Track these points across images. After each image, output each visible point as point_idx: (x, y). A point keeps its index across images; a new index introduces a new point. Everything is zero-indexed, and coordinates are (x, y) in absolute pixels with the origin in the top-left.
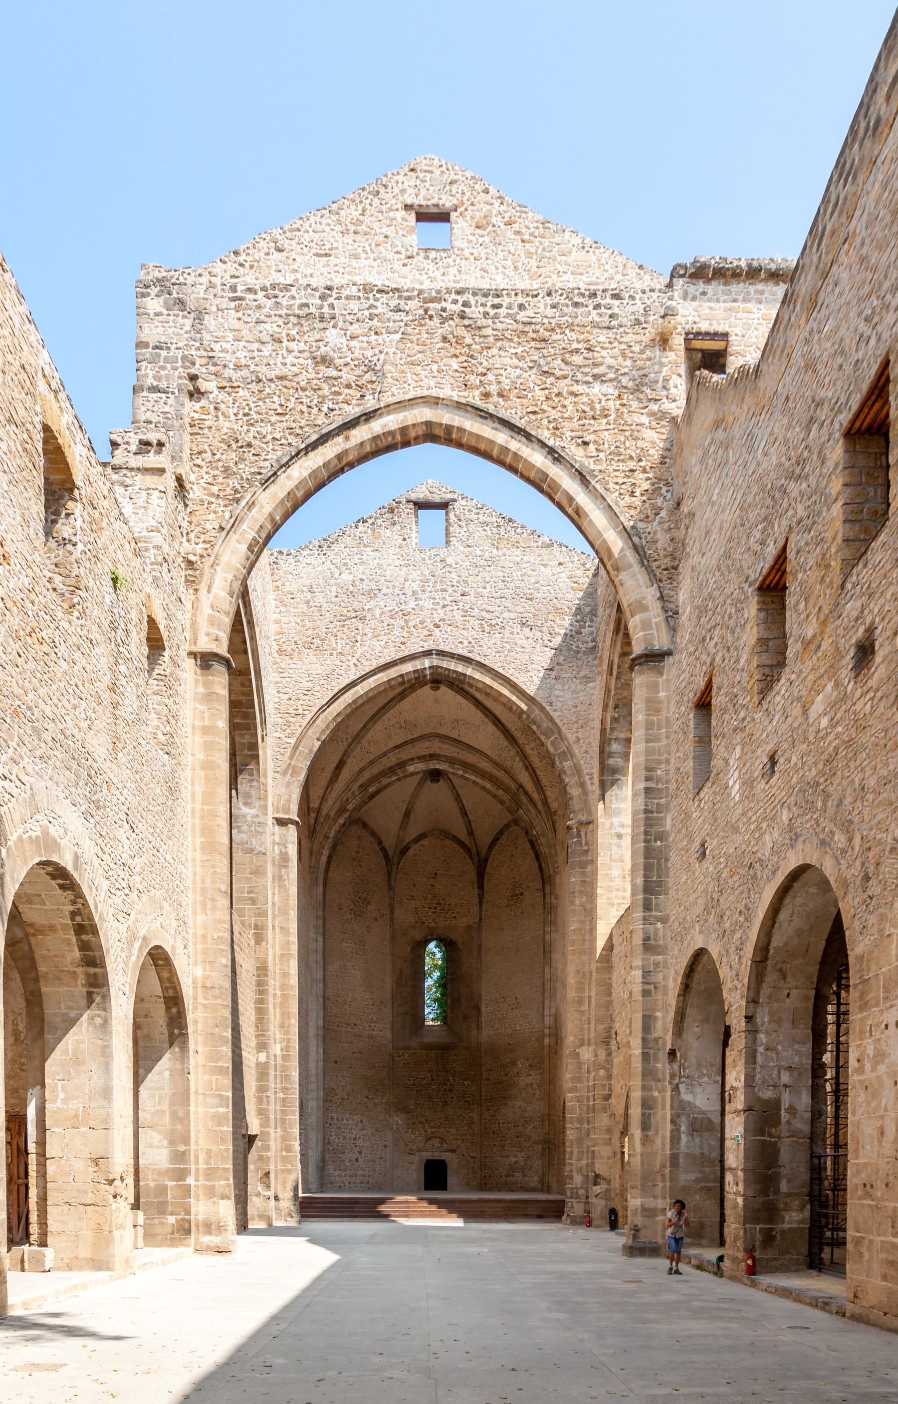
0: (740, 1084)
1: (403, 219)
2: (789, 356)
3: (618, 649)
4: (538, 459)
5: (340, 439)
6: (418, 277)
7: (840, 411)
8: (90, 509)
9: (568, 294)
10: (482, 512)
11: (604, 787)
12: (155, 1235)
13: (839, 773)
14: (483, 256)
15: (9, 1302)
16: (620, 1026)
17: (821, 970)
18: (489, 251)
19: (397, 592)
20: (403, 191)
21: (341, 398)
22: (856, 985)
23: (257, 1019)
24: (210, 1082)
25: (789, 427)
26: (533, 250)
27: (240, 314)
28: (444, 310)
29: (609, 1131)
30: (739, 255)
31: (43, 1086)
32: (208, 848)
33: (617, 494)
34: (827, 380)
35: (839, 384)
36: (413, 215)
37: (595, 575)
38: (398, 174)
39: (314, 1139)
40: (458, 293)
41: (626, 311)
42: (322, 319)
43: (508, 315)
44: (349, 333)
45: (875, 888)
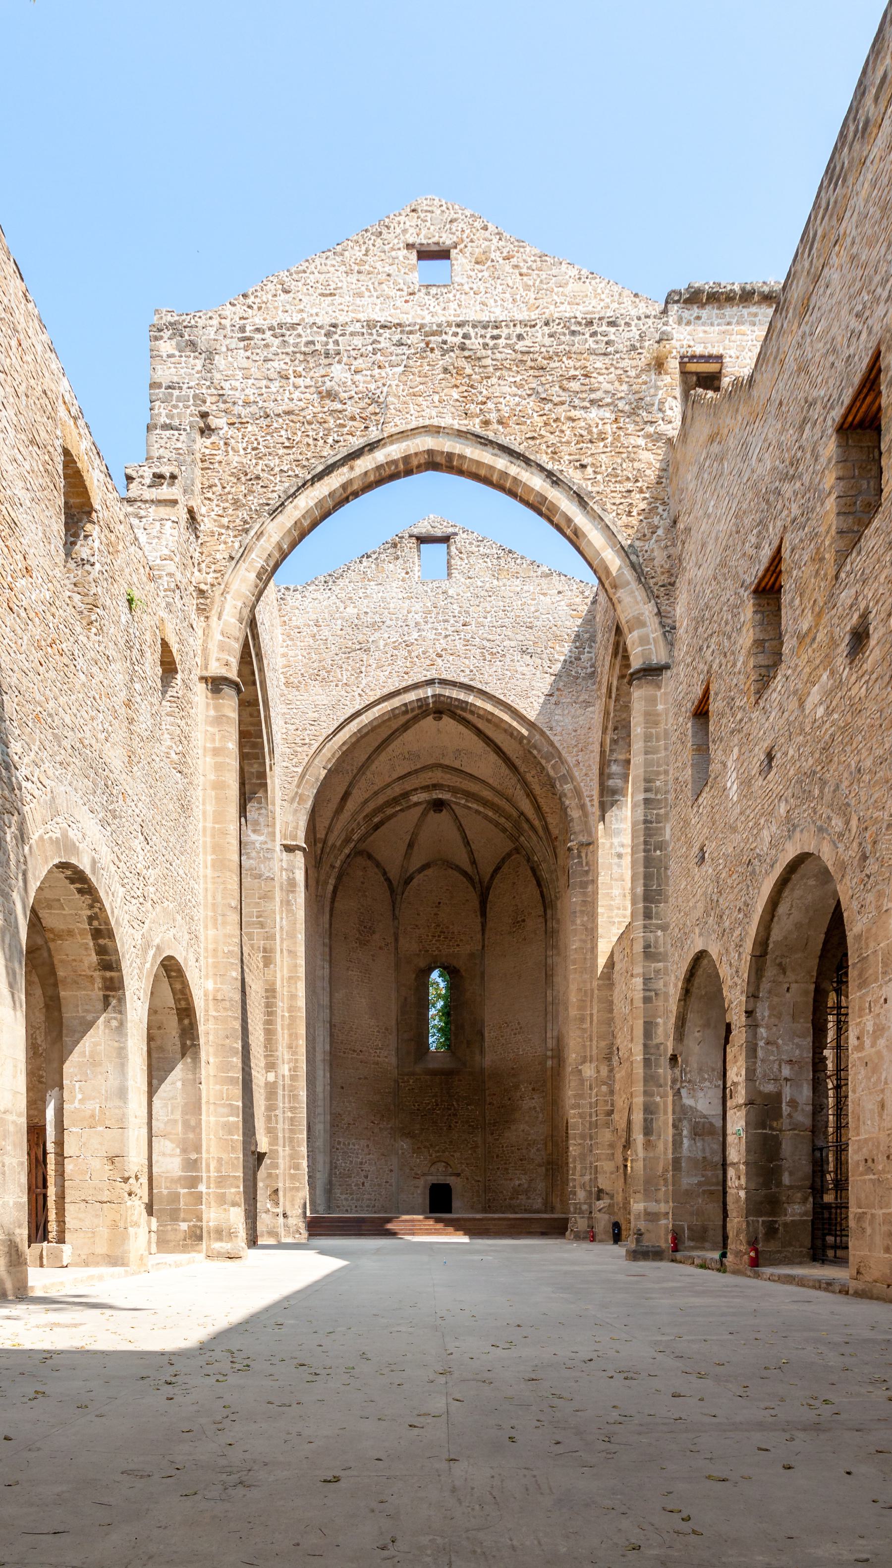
0: (741, 1079)
1: (405, 258)
2: (782, 362)
3: (617, 672)
4: (537, 482)
5: (345, 469)
6: (419, 312)
7: (832, 407)
8: (107, 532)
9: (565, 322)
10: (482, 544)
11: (604, 808)
12: (168, 1242)
13: (836, 759)
14: (483, 290)
15: (30, 1284)
16: (621, 1041)
17: (820, 965)
18: (488, 285)
19: (400, 623)
21: (345, 430)
22: (854, 964)
23: (266, 1039)
24: (221, 1091)
25: (783, 430)
26: (531, 283)
27: (249, 354)
28: (445, 342)
29: (612, 1146)
30: (733, 279)
31: (61, 1088)
32: (219, 865)
33: (614, 514)
34: (819, 380)
35: (831, 382)
36: (415, 253)
37: (594, 602)
38: (400, 215)
39: (321, 1162)
40: (458, 325)
41: (621, 337)
42: (327, 355)
43: (507, 346)
44: (353, 368)
45: (872, 866)
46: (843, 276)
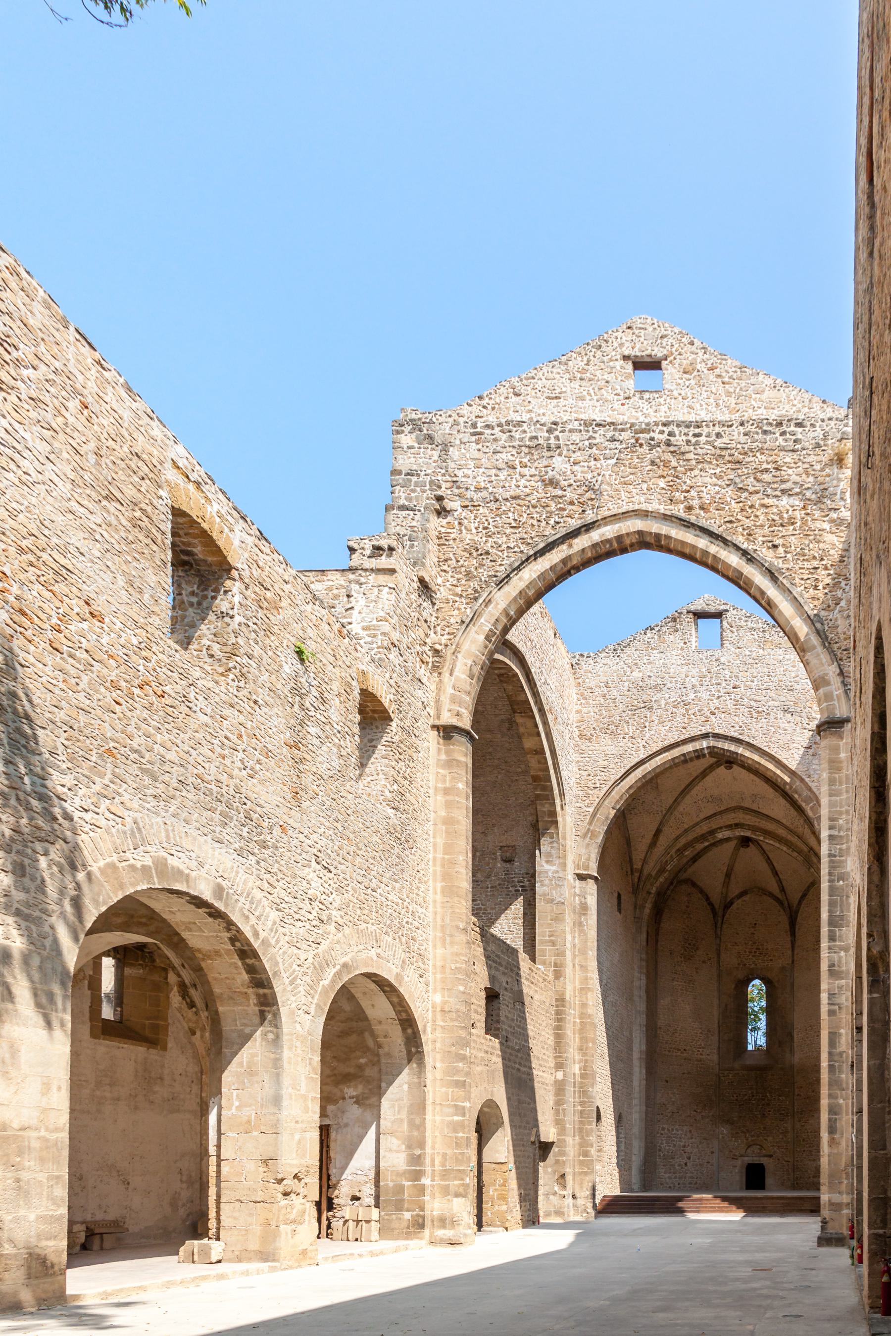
14: (690, 395)
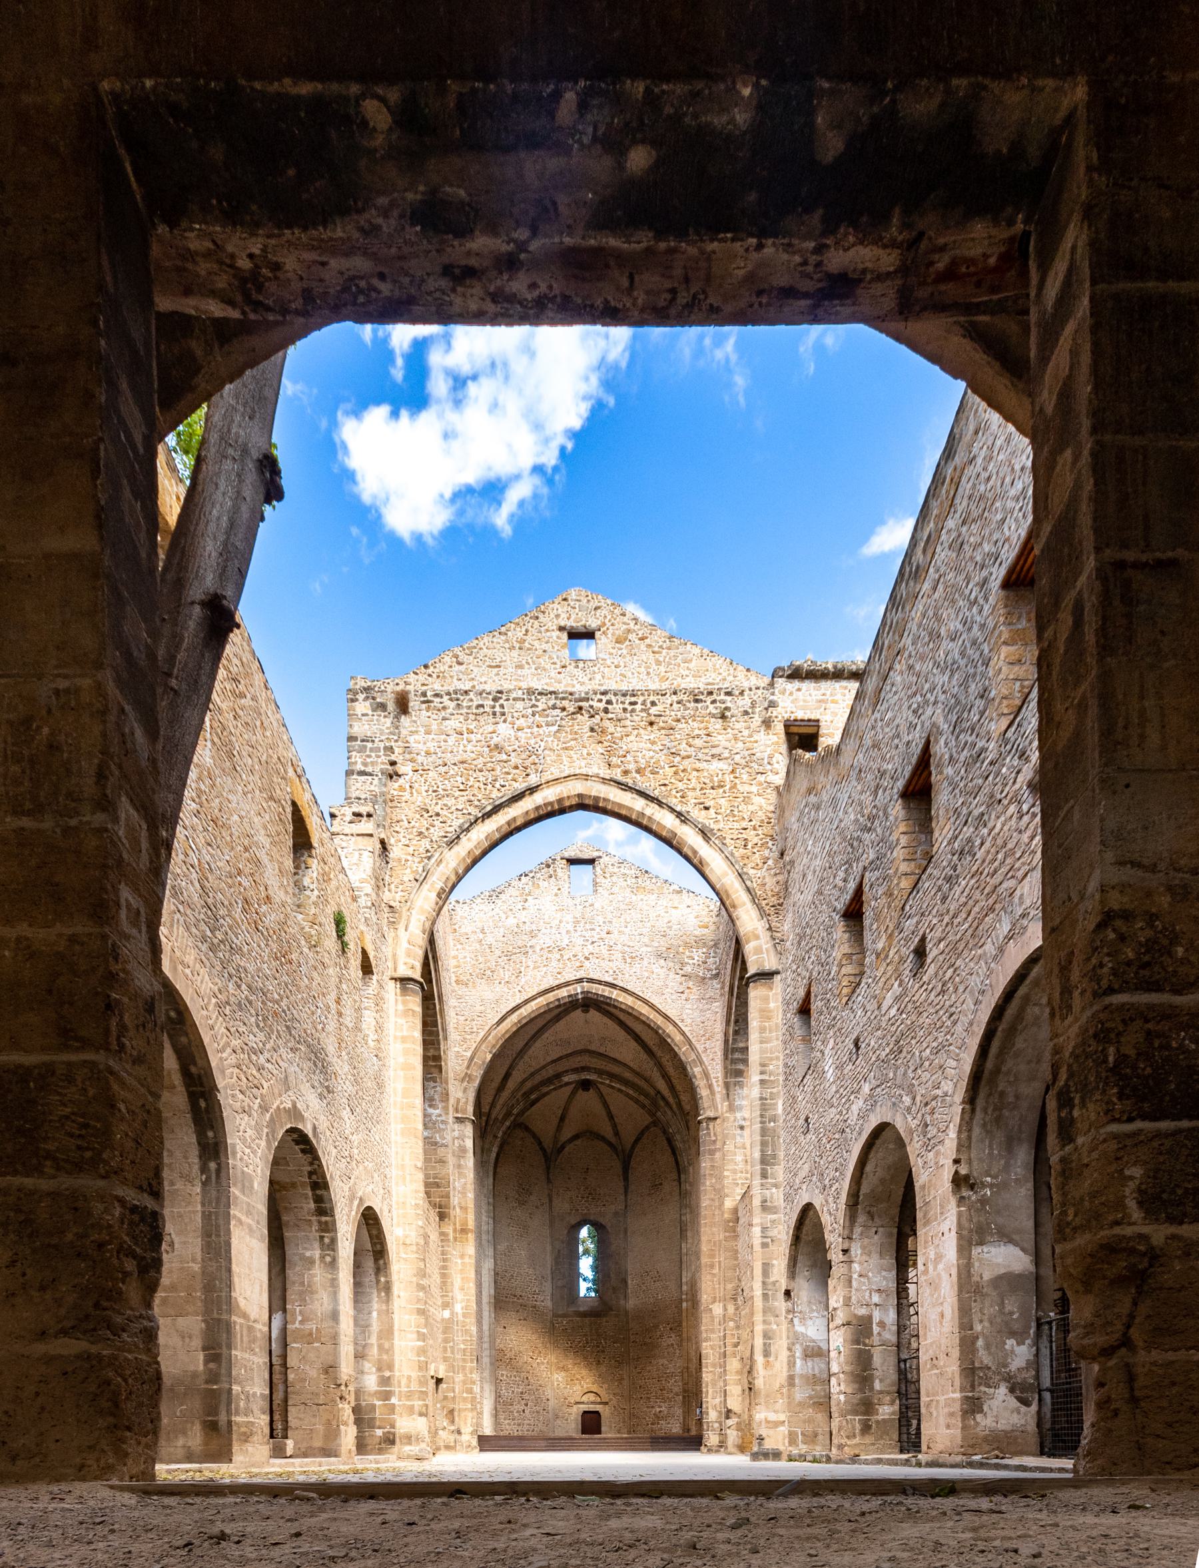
4: (667, 820)
20: (557, 616)
21: (510, 777)
27: (429, 714)
46: (904, 680)
